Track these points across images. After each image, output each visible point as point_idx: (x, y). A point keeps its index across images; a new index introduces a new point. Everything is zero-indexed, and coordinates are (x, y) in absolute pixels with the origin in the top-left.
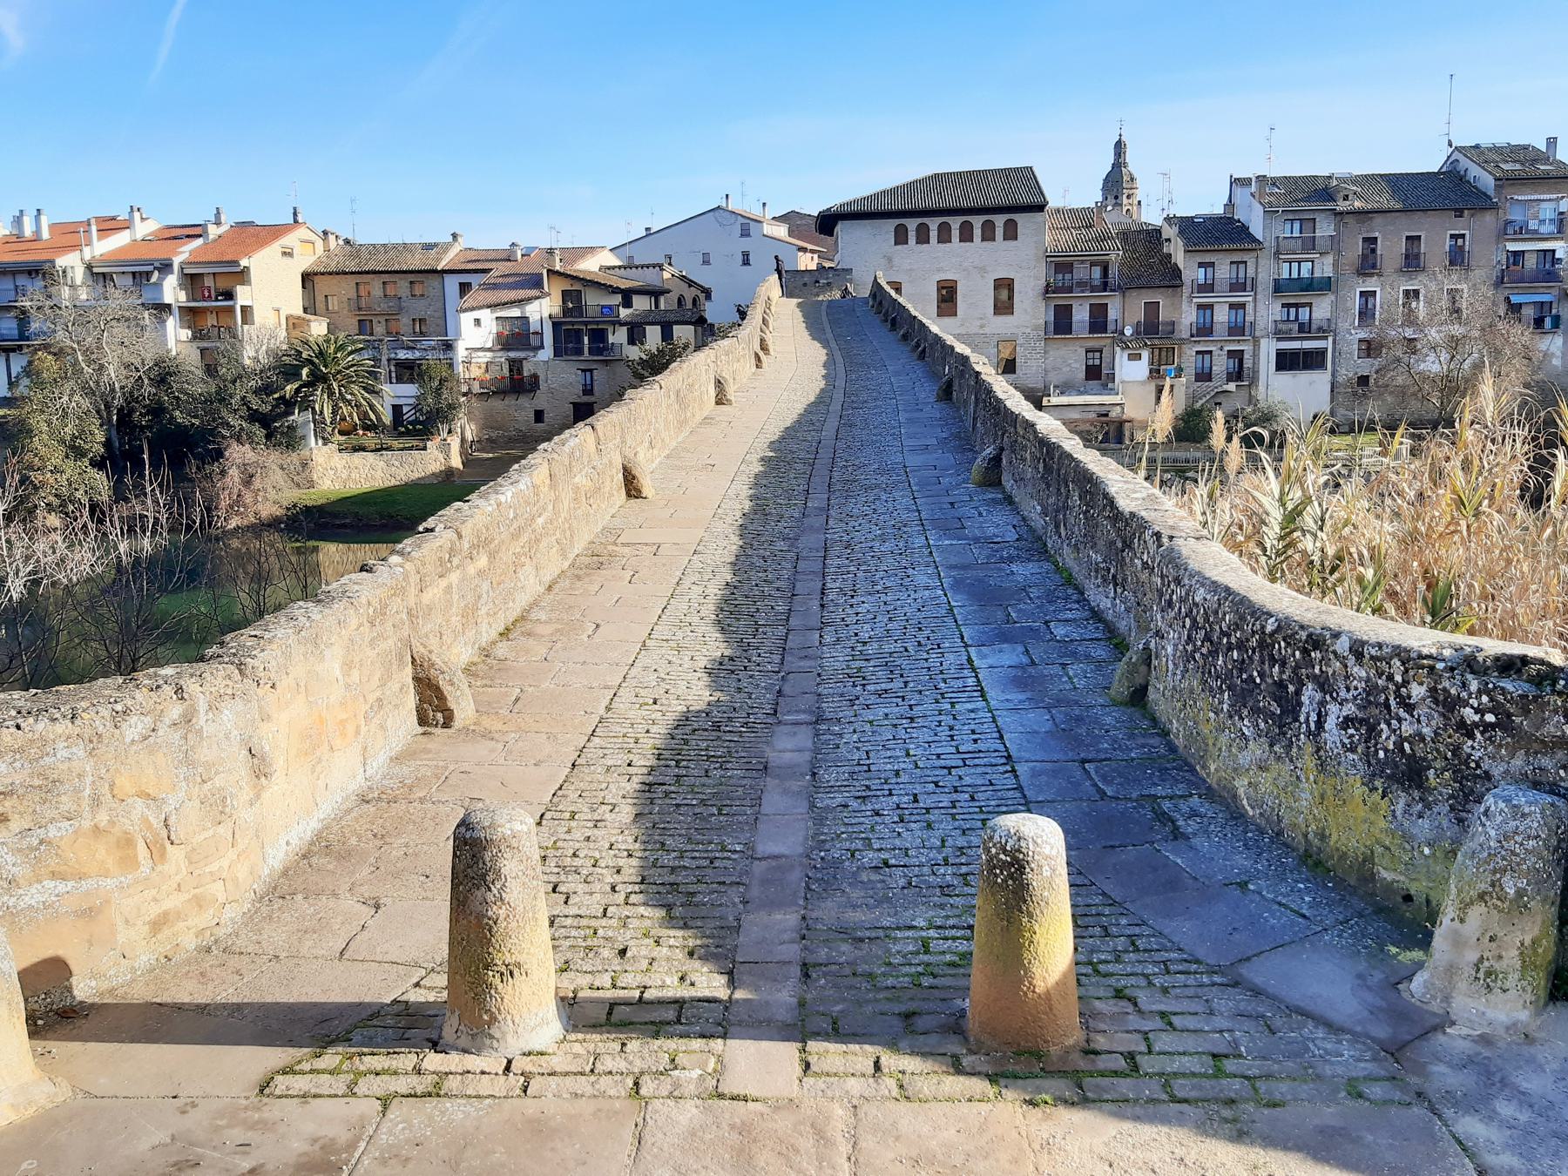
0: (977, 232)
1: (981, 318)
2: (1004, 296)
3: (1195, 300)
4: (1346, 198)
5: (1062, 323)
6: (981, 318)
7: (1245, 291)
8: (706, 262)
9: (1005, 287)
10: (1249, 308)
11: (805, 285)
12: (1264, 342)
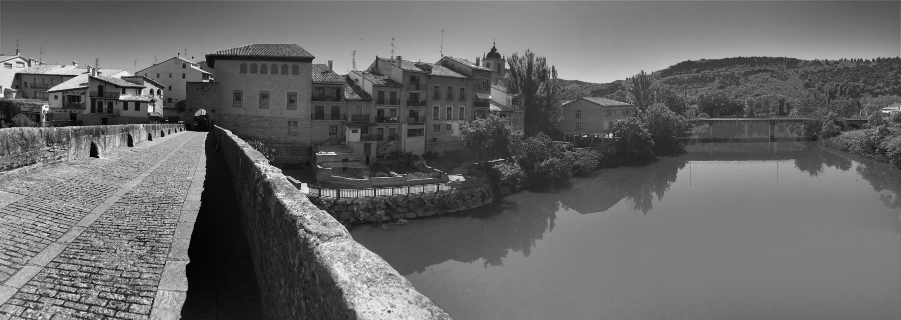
0: (280, 70)
1: (281, 110)
5: (318, 115)
6: (281, 110)
7: (396, 104)
8: (158, 76)
10: (397, 112)
12: (404, 126)
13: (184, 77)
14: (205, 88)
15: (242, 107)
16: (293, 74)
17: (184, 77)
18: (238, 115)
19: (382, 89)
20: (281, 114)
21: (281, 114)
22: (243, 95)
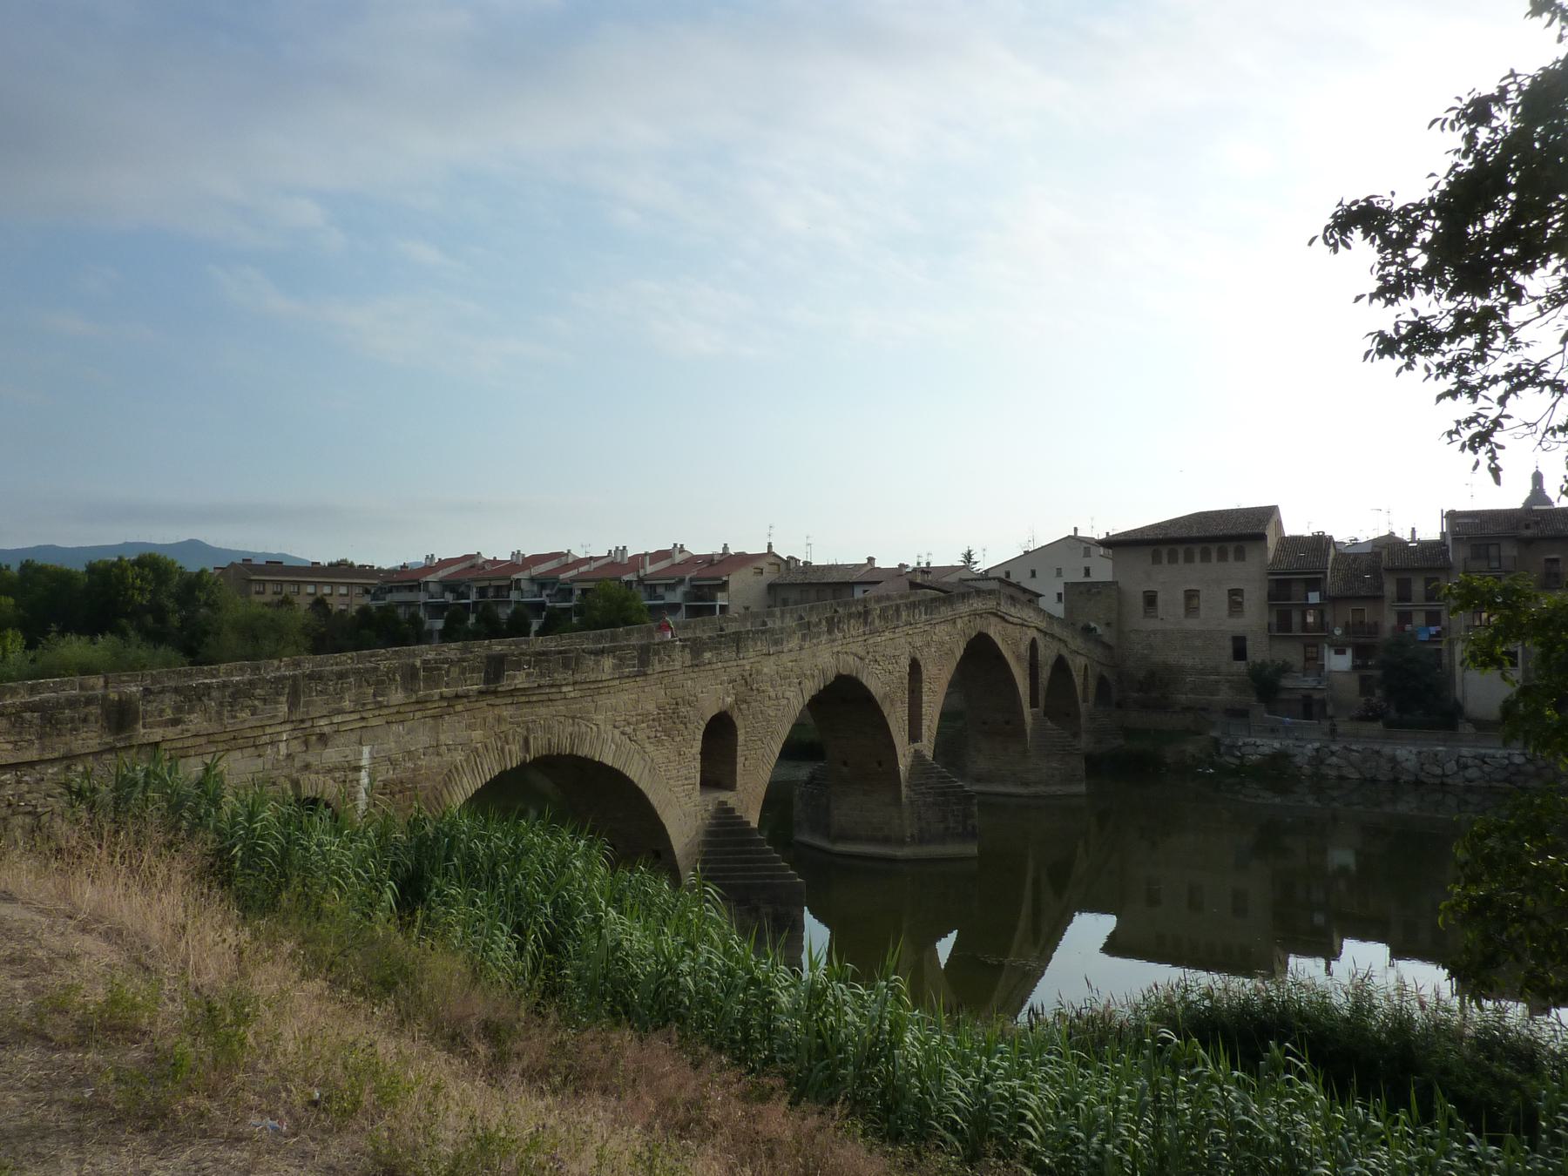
2: (1235, 600)
4: (1527, 527)
8: (1033, 574)
9: (1235, 593)
13: (1059, 572)
14: (1094, 590)
17: (1059, 572)
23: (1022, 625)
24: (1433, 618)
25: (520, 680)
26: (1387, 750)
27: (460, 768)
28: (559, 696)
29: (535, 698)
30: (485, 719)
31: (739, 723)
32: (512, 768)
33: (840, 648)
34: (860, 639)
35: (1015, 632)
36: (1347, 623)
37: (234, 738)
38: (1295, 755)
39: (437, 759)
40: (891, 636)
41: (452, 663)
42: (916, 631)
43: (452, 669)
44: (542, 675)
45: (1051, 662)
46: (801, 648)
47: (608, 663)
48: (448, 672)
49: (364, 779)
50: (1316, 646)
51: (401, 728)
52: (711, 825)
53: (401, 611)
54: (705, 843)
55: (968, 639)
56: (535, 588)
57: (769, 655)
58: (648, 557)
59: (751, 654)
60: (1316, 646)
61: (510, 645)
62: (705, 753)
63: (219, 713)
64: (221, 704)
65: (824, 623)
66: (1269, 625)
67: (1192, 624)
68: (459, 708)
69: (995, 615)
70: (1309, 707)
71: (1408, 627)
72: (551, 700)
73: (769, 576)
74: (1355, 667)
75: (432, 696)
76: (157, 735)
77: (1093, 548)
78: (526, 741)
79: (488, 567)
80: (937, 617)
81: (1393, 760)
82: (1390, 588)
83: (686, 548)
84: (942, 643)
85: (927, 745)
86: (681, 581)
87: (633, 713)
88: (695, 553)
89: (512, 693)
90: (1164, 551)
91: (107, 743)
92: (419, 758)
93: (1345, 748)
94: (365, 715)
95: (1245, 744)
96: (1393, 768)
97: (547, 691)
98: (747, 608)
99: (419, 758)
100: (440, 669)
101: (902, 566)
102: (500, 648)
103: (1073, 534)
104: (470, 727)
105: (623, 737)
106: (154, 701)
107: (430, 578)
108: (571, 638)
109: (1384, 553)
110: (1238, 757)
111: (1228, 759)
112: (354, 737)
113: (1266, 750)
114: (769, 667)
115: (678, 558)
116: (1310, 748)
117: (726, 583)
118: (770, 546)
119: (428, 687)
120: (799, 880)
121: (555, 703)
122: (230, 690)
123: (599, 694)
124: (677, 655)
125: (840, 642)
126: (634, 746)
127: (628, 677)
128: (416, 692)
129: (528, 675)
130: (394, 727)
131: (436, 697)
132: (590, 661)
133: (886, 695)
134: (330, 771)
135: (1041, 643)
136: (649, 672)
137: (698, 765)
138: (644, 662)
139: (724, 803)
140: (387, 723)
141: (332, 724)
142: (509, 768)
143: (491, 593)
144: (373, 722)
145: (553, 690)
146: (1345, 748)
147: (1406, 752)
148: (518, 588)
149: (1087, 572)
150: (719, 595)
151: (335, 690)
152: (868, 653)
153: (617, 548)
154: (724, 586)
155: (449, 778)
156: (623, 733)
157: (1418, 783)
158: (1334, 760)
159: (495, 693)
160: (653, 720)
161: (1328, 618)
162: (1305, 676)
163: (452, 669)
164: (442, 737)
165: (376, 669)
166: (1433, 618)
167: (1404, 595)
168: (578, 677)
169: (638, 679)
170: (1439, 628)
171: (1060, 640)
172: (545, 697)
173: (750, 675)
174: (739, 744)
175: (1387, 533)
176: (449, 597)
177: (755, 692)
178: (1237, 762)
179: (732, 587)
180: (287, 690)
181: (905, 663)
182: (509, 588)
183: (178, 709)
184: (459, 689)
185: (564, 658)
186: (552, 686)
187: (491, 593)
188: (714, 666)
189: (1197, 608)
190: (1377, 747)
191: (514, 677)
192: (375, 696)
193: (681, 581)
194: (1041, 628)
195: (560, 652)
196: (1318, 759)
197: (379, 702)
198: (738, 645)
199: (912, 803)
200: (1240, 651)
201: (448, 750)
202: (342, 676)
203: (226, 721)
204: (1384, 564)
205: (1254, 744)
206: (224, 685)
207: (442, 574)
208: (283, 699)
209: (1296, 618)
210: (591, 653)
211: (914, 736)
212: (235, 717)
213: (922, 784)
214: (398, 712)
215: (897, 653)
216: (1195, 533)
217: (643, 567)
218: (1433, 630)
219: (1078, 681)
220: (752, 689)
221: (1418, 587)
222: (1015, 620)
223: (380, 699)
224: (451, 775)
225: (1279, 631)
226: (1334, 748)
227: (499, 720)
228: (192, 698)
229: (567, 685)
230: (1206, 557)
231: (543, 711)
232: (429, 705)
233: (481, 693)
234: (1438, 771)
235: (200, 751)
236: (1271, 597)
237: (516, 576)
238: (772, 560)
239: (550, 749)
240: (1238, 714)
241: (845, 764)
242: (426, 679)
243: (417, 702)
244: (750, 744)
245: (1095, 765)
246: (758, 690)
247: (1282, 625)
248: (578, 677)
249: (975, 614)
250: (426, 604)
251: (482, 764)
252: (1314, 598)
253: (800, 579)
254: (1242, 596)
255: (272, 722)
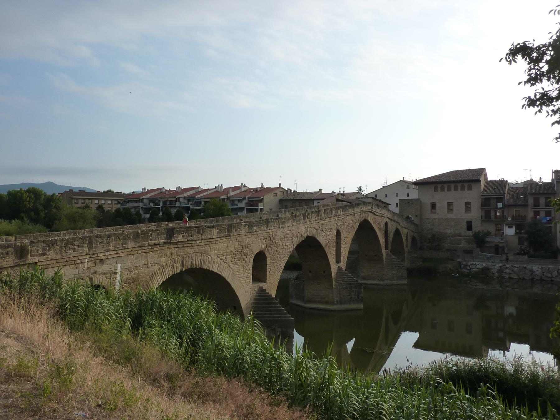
3: (532, 210)
8: (386, 196)
9: (468, 204)
11: (405, 203)
13: (397, 195)
14: (411, 202)
15: (436, 213)
16: (441, 191)
17: (397, 195)
18: (434, 219)
19: (537, 196)
20: (461, 216)
21: (461, 216)
22: (437, 205)
23: (382, 216)
24: (548, 213)
25: (180, 238)
26: (529, 267)
27: (156, 273)
28: (196, 245)
29: (186, 245)
30: (166, 254)
31: (268, 255)
32: (177, 273)
33: (308, 225)
34: (316, 222)
35: (379, 219)
36: (513, 215)
37: (67, 261)
38: (491, 269)
39: (147, 269)
40: (329, 221)
41: (153, 231)
42: (339, 218)
43: (153, 234)
44: (189, 236)
45: (393, 231)
46: (293, 225)
47: (215, 231)
48: (151, 235)
49: (118, 278)
50: (501, 225)
51: (133, 257)
52: (256, 296)
53: (132, 210)
54: (254, 303)
55: (360, 222)
56: (186, 201)
57: (280, 228)
58: (231, 189)
59: (273, 228)
60: (501, 225)
61: (176, 224)
62: (253, 267)
63: (61, 251)
64: (61, 247)
65: (302, 215)
66: (481, 216)
67: (451, 216)
68: (156, 249)
69: (371, 212)
70: (497, 250)
71: (538, 217)
72: (193, 246)
73: (280, 196)
74: (516, 233)
75: (145, 244)
76: (36, 259)
77: (410, 186)
78: (183, 262)
79: (167, 193)
80: (347, 213)
81: (532, 271)
82: (531, 201)
83: (246, 185)
84: (349, 224)
85: (343, 265)
86: (245, 198)
87: (225, 251)
88: (250, 187)
89: (176, 243)
90: (439, 186)
91: (17, 263)
92: (140, 269)
93: (512, 266)
94: (118, 252)
95: (471, 264)
96: (531, 274)
97: (191, 242)
98: (271, 209)
99: (140, 269)
100: (148, 233)
101: (333, 192)
102: (172, 225)
103: (402, 179)
104: (160, 257)
105: (221, 261)
106: (35, 246)
107: (144, 197)
108: (200, 221)
109: (529, 187)
110: (468, 269)
111: (464, 270)
112: (114, 260)
113: (480, 267)
114: (280, 233)
115: (243, 189)
116: (498, 266)
117: (262, 199)
118: (280, 184)
119: (144, 241)
120: (291, 318)
121: (194, 247)
122: (65, 242)
123: (211, 244)
124: (243, 228)
125: (308, 223)
126: (226, 264)
127: (223, 237)
128: (139, 243)
129: (183, 236)
130: (130, 257)
131: (147, 245)
132: (208, 230)
133: (327, 245)
134: (104, 274)
135: (389, 224)
136: (232, 235)
137: (251, 272)
138: (230, 231)
139: (262, 287)
140: (127, 255)
141: (105, 255)
142: (176, 273)
143: (168, 203)
144: (122, 255)
145: (193, 242)
146: (512, 266)
147: (537, 268)
148: (179, 201)
149: (408, 195)
150: (260, 204)
151: (106, 242)
152: (319, 227)
153: (219, 185)
154: (261, 201)
155: (152, 277)
156: (221, 259)
157: (542, 280)
158: (507, 271)
159: (170, 243)
160: (233, 254)
161: (505, 214)
162: (496, 237)
163: (153, 234)
164: (149, 261)
165: (123, 234)
166: (548, 213)
167: (536, 204)
168: (203, 237)
169: (227, 238)
170: (550, 218)
171: (397, 222)
172: (190, 245)
173: (272, 236)
174: (268, 264)
175: (530, 179)
176: (152, 205)
177: (274, 243)
178: (468, 271)
179: (265, 200)
180: (87, 242)
181: (334, 231)
182: (175, 201)
183: (44, 249)
184: (156, 241)
185: (197, 229)
186: (193, 240)
187: (168, 203)
188: (258, 233)
189: (452, 210)
190: (525, 266)
191: (178, 237)
192: (122, 244)
193: (245, 198)
194: (390, 217)
195: (196, 227)
196: (501, 271)
197: (124, 247)
198: (267, 224)
199: (337, 288)
200: (469, 226)
201: (152, 266)
202: (109, 236)
203: (63, 254)
204: (528, 192)
205: (475, 264)
206: (62, 240)
207: (149, 195)
208: (86, 245)
209: (492, 213)
210: (209, 227)
211: (338, 261)
212: (67, 253)
213: (341, 280)
214: (132, 251)
215: (331, 227)
216: (451, 179)
217: (229, 193)
218: (548, 218)
219: (404, 239)
220: (273, 242)
221: (542, 201)
222: (379, 214)
223: (124, 245)
224: (153, 276)
225: (485, 219)
226: (507, 266)
227: (172, 254)
228: (51, 244)
229: (199, 240)
230: (456, 189)
231: (189, 250)
232: (144, 248)
233: (164, 243)
234: (550, 275)
235: (53, 266)
236: (483, 205)
237: (178, 197)
238: (281, 190)
239: (192, 265)
240: (468, 252)
241: (310, 272)
242: (142, 238)
243: (139, 247)
244: (272, 264)
245: (410, 272)
246: (275, 242)
247: (487, 216)
248: (203, 237)
249: (362, 212)
250: (142, 208)
251: (165, 271)
252: (500, 205)
253: (292, 198)
254: (471, 205)
255: (81, 255)
